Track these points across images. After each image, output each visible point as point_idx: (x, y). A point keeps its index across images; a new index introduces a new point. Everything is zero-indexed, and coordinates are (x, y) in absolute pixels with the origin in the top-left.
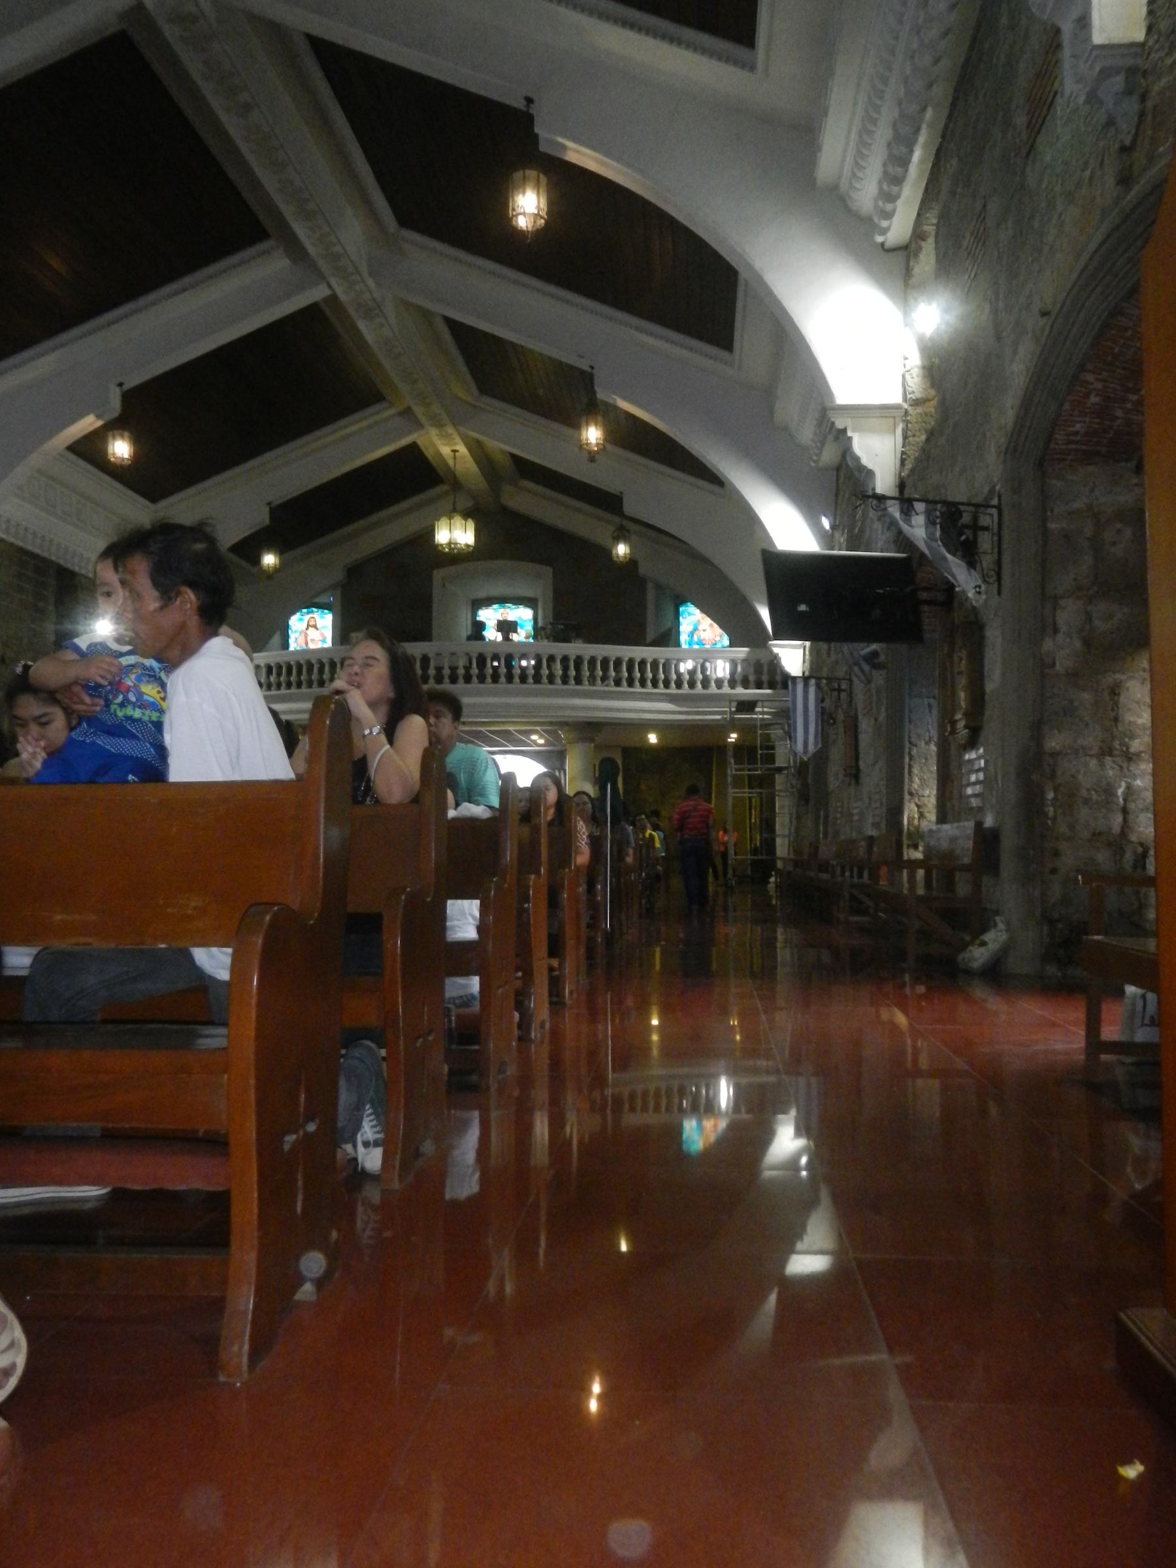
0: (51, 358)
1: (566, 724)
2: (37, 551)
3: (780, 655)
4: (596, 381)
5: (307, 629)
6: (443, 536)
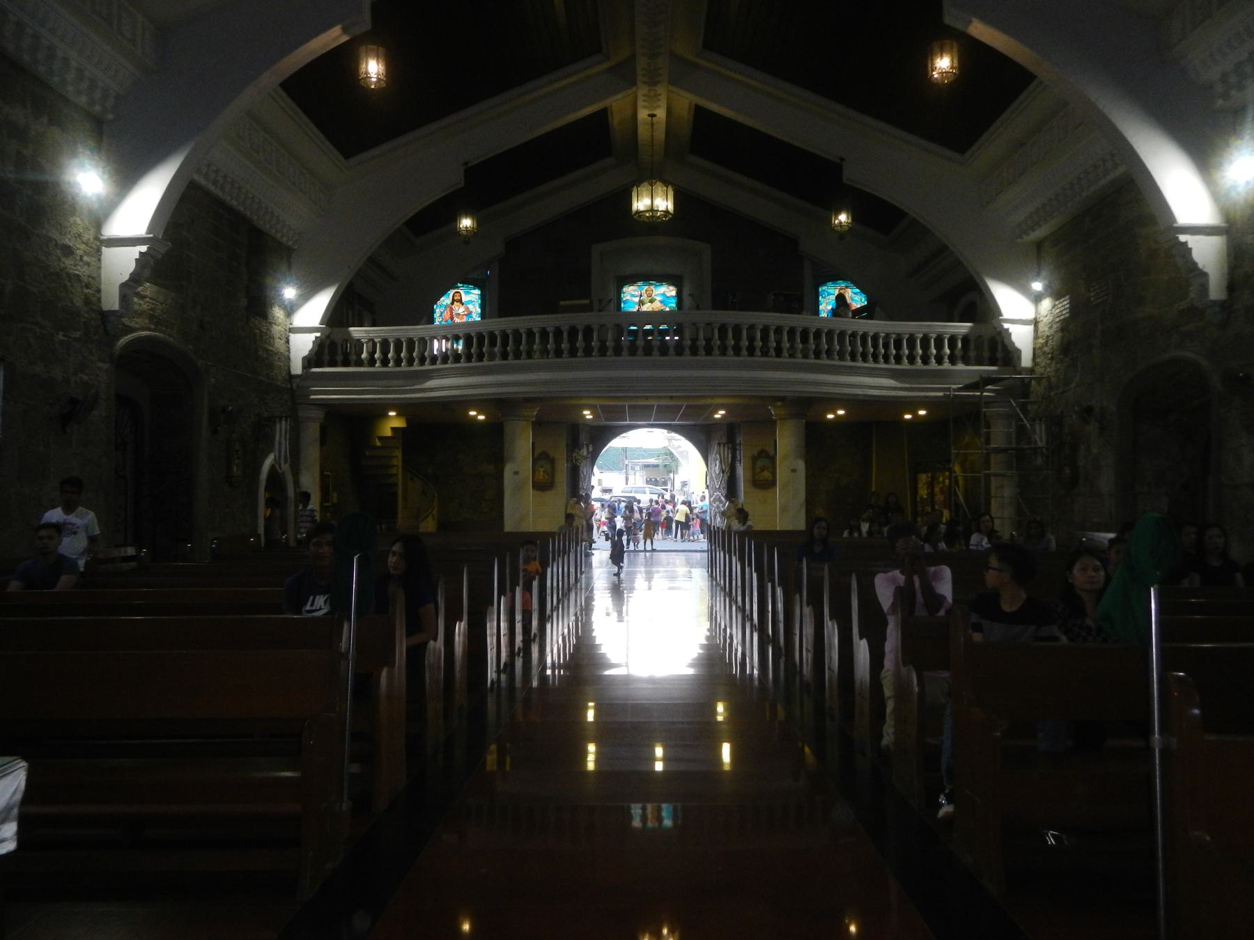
1: (782, 399)
3: (1010, 331)
5: (452, 303)
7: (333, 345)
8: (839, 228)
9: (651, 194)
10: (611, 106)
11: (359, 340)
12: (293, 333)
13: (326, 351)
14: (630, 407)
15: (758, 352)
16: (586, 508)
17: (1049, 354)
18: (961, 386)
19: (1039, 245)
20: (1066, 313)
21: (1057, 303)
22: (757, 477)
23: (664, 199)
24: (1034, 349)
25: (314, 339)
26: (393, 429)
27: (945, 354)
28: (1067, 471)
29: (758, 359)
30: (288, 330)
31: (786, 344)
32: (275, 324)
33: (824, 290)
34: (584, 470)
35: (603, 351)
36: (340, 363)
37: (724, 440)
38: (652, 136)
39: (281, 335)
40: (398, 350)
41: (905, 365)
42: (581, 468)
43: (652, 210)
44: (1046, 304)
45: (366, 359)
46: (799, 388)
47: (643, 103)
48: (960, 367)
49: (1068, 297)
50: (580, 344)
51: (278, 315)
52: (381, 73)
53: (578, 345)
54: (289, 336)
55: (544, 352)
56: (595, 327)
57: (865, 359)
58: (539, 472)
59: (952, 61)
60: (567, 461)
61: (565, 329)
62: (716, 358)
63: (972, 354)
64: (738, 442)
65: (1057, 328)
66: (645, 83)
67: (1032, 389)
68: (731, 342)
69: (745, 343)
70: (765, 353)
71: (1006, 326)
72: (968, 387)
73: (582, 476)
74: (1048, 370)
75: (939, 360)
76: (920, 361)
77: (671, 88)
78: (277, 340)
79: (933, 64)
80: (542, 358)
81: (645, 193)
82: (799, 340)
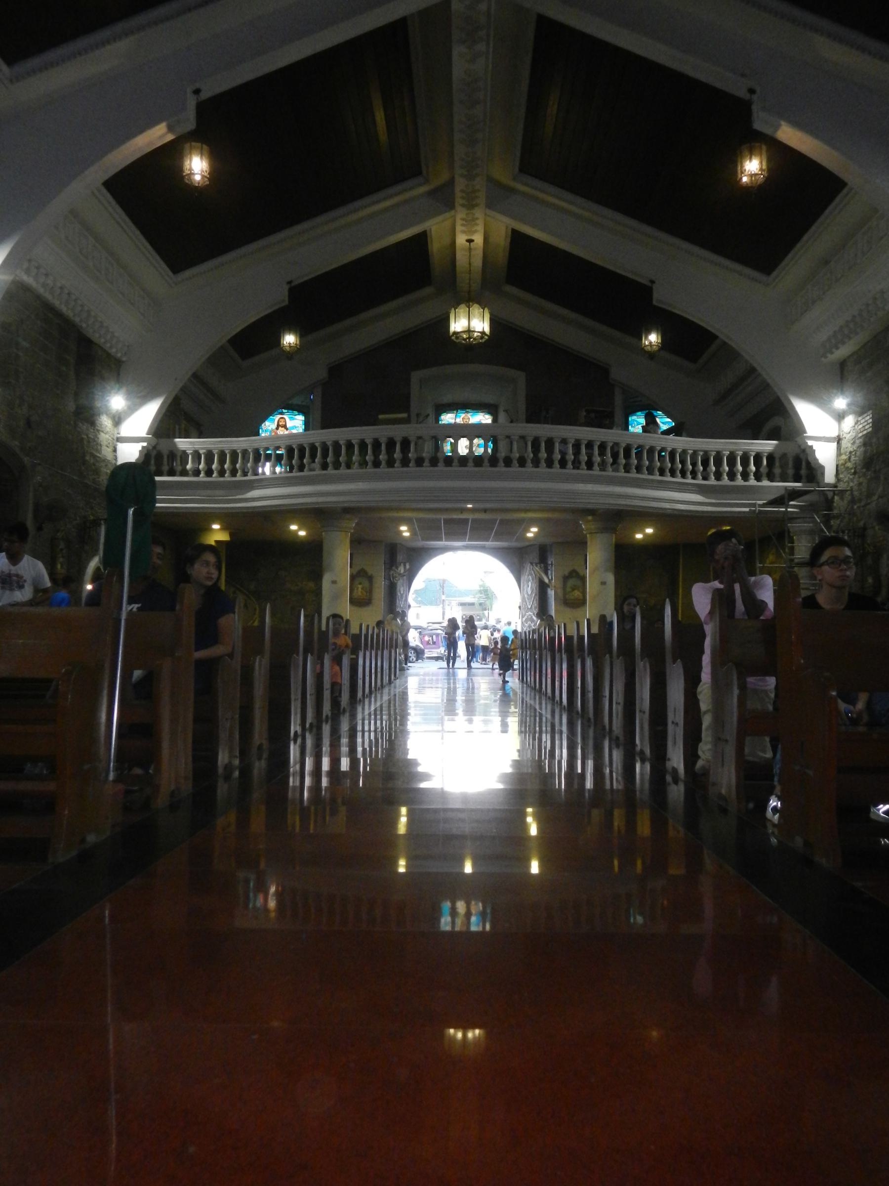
0: (122, 46)
1: (592, 512)
2: (64, 309)
4: (755, 108)
5: (277, 429)
6: (458, 325)
7: (159, 457)
8: (649, 348)
9: (468, 318)
10: (431, 230)
11: (184, 452)
12: (121, 442)
13: (153, 462)
14: (447, 521)
15: (570, 465)
16: (402, 624)
17: (851, 469)
18: (765, 502)
19: (843, 365)
20: (869, 428)
21: (860, 419)
22: (567, 596)
23: (480, 321)
24: (837, 466)
25: (140, 449)
26: (216, 542)
27: (751, 471)
28: (870, 580)
29: (570, 470)
30: (115, 438)
31: (597, 459)
32: (103, 432)
33: (634, 420)
34: (401, 589)
35: (420, 462)
36: (165, 473)
37: (537, 560)
38: (470, 264)
39: (109, 443)
40: (222, 461)
41: (712, 481)
42: (398, 589)
43: (469, 331)
44: (849, 421)
45: (191, 469)
46: (612, 501)
47: (464, 228)
48: (765, 483)
49: (871, 412)
50: (397, 455)
51: (106, 423)
52: (204, 170)
53: (395, 456)
54: (116, 445)
55: (363, 464)
56: (412, 439)
57: (673, 473)
58: (358, 589)
59: (761, 163)
60: (384, 578)
61: (383, 441)
62: (529, 468)
63: (777, 471)
64: (550, 563)
65: (860, 443)
66: (463, 206)
67: (835, 504)
68: (543, 455)
69: (557, 456)
70: (576, 464)
71: (810, 443)
72: (772, 503)
73: (399, 594)
74: (851, 484)
75: (745, 476)
76: (726, 478)
77: (488, 212)
78: (104, 448)
79: (742, 166)
80: (362, 468)
81: (462, 314)
82: (610, 455)
